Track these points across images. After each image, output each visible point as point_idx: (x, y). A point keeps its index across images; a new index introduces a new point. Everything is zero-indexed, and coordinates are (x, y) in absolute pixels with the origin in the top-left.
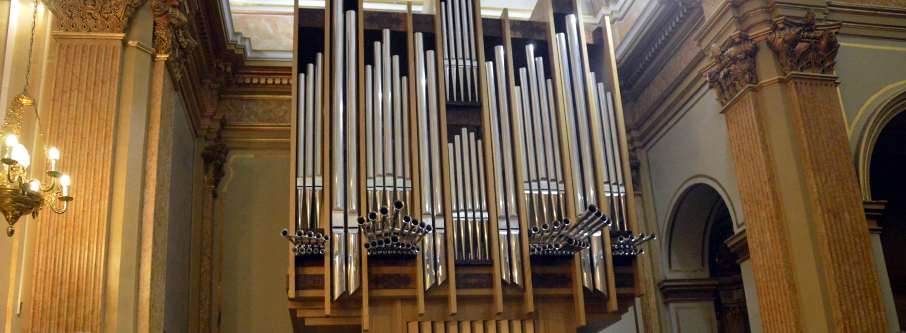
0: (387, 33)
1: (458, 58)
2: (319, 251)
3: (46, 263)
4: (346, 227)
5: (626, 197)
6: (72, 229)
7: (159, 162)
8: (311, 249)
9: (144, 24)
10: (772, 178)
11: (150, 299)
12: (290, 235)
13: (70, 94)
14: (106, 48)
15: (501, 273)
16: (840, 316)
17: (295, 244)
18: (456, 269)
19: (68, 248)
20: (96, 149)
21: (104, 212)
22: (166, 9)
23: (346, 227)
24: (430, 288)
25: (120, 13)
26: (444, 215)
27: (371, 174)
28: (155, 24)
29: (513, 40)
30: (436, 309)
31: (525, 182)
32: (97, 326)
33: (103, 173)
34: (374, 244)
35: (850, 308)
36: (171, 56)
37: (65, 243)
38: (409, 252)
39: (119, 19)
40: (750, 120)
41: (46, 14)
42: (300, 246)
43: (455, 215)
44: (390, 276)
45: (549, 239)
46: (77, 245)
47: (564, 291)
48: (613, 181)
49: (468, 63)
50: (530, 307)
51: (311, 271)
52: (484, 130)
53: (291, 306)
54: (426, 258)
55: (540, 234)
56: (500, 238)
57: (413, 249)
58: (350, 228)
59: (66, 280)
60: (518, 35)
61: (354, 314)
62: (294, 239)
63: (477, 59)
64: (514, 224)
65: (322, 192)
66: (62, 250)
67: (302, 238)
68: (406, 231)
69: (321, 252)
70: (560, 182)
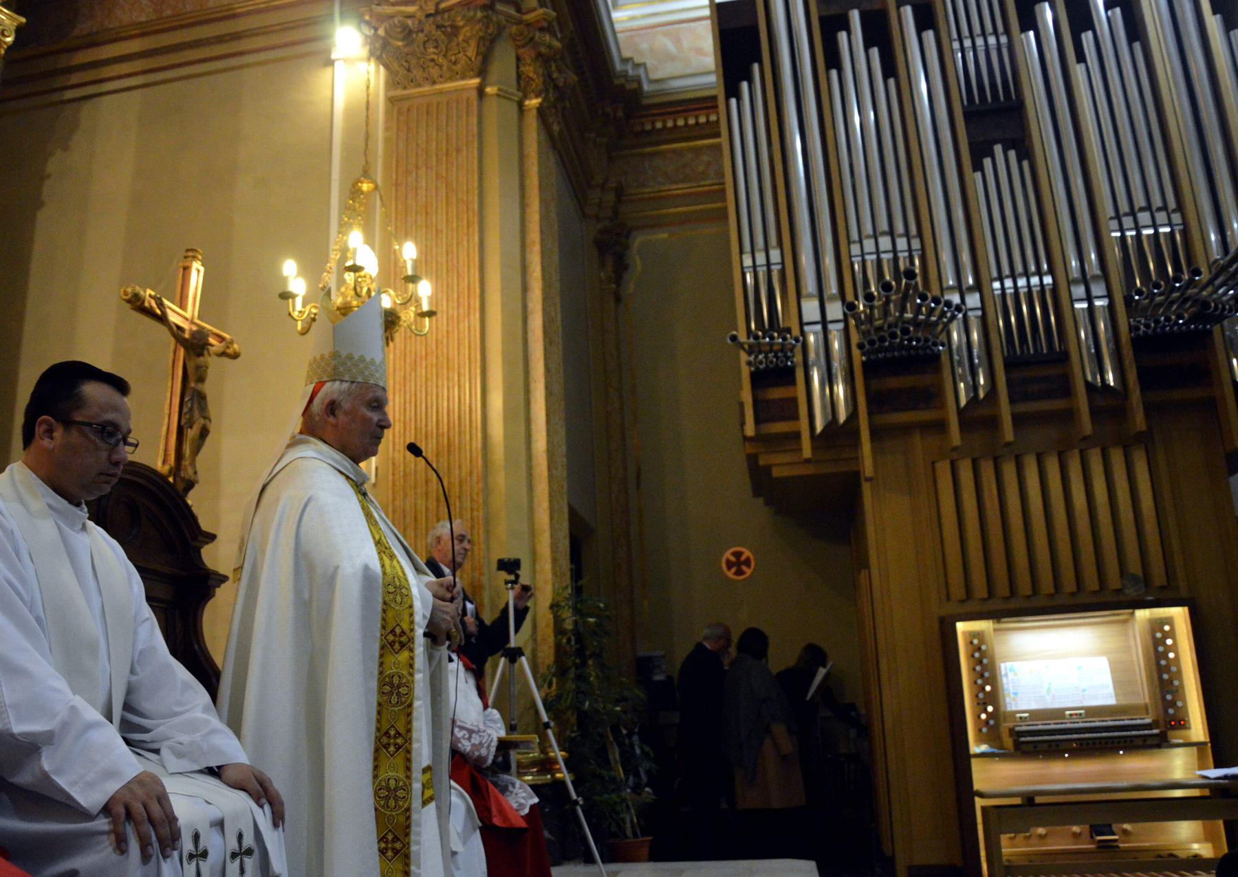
0: (855, 16)
1: (975, 34)
2: (787, 362)
3: (405, 410)
4: (824, 322)
6: (435, 358)
7: (542, 253)
8: (775, 360)
9: (504, 62)
11: (548, 450)
13: (417, 173)
14: (458, 102)
17: (750, 354)
19: (432, 387)
20: (458, 244)
21: (475, 331)
22: (530, 36)
23: (824, 322)
25: (471, 52)
26: (978, 287)
27: (855, 235)
28: (518, 59)
31: (1111, 218)
32: (478, 494)
33: (469, 276)
34: (872, 343)
36: (544, 100)
37: (426, 380)
38: (928, 351)
39: (470, 60)
41: (377, 71)
42: (756, 357)
43: (997, 285)
45: (1165, 306)
46: (442, 381)
51: (776, 393)
52: (1031, 141)
53: (750, 449)
54: (956, 357)
55: (1147, 301)
56: (1076, 312)
57: (935, 344)
58: (832, 322)
59: (432, 431)
62: (746, 346)
63: (1007, 31)
64: (1098, 289)
65: (783, 272)
66: (424, 390)
68: (921, 317)
70: (1174, 211)
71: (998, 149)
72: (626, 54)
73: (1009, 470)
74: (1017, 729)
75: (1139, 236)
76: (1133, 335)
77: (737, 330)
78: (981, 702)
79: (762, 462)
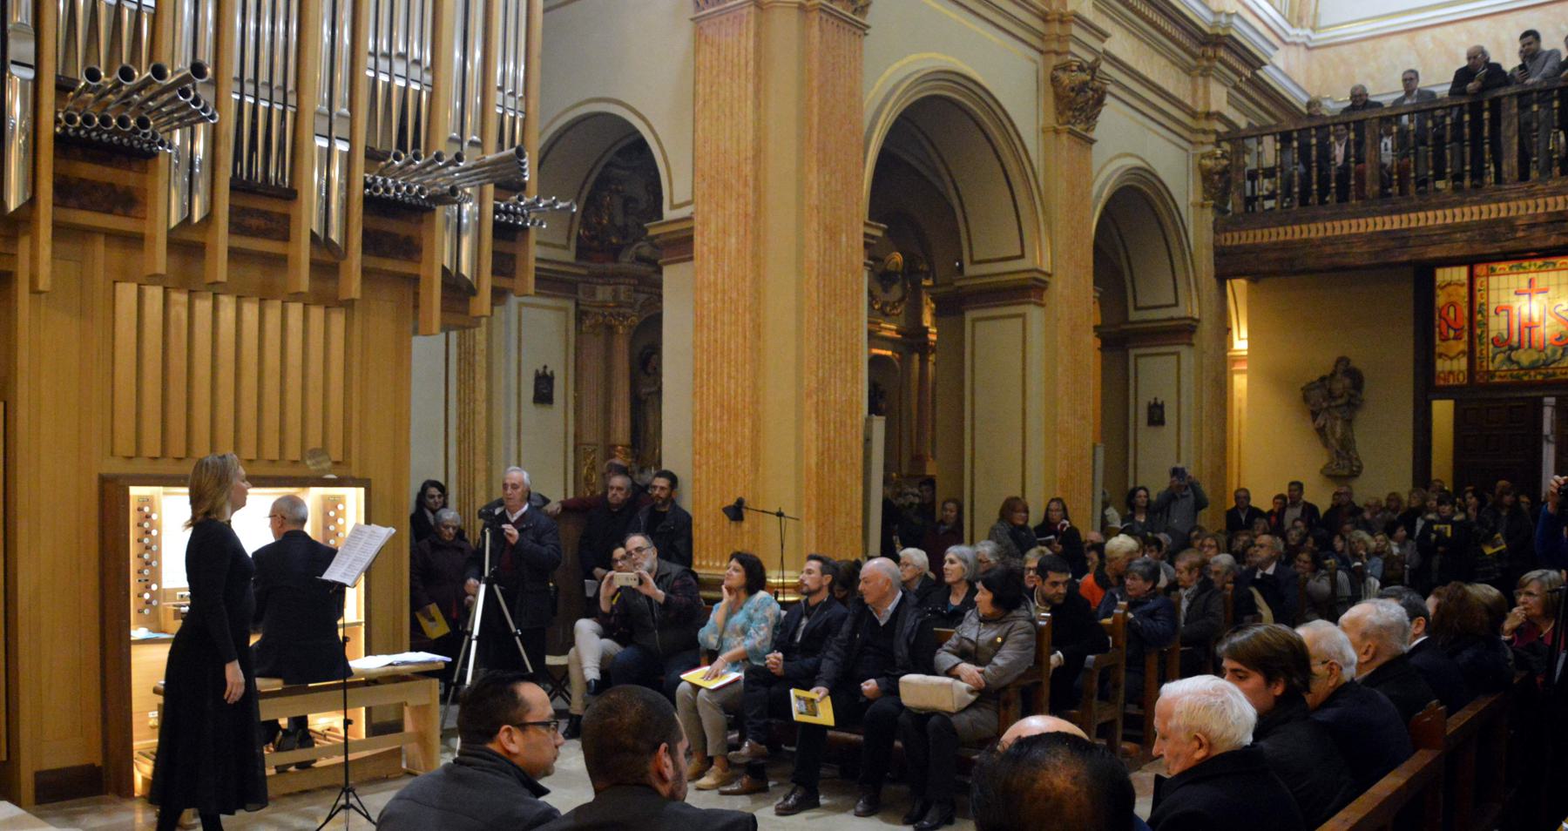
10: (758, 154)
15: (309, 219)
16: (814, 385)
18: (231, 195)
31: (370, 54)
35: (827, 375)
40: (743, 52)
44: (94, 186)
50: (353, 289)
64: (340, 128)
75: (389, 87)
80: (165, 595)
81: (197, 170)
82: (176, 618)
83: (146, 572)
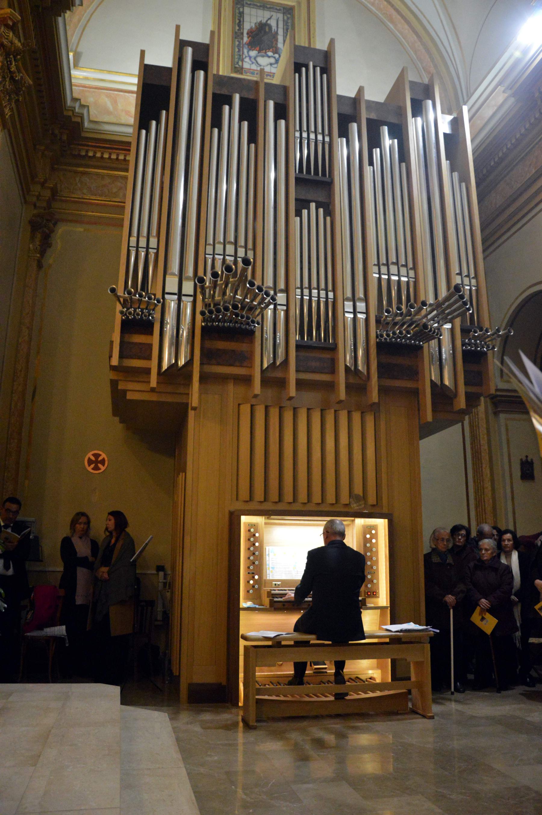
0: (237, 98)
2: (149, 316)
4: (180, 294)
5: (477, 291)
12: (118, 294)
18: (297, 351)
23: (180, 294)
24: (267, 367)
29: (369, 121)
30: (270, 393)
31: (375, 265)
34: (211, 312)
47: (409, 384)
48: (465, 273)
49: (320, 137)
52: (334, 205)
57: (253, 322)
60: (373, 116)
61: (182, 390)
62: (122, 300)
63: (330, 134)
64: (361, 306)
67: (131, 299)
69: (150, 318)
70: (411, 269)
71: (313, 205)
72: (75, 95)
73: (288, 416)
74: (273, 592)
75: (389, 280)
76: (378, 340)
77: (117, 286)
78: (251, 572)
79: (119, 388)
80: (265, 583)
81: (278, 341)
82: (268, 597)
83: (251, 567)
